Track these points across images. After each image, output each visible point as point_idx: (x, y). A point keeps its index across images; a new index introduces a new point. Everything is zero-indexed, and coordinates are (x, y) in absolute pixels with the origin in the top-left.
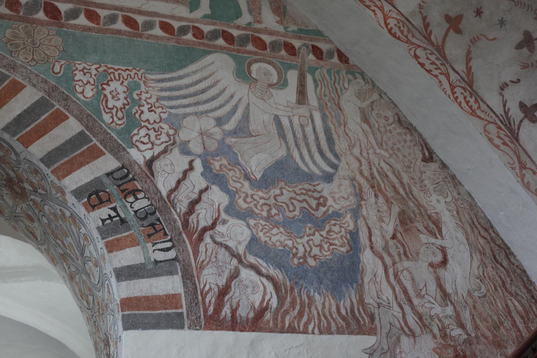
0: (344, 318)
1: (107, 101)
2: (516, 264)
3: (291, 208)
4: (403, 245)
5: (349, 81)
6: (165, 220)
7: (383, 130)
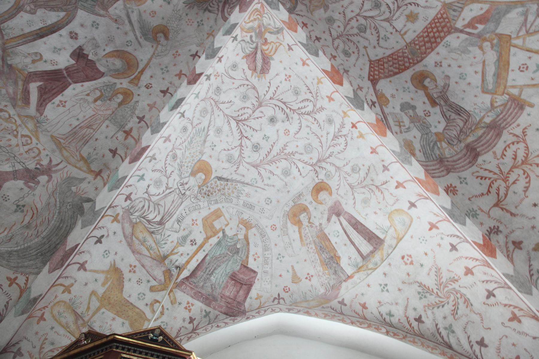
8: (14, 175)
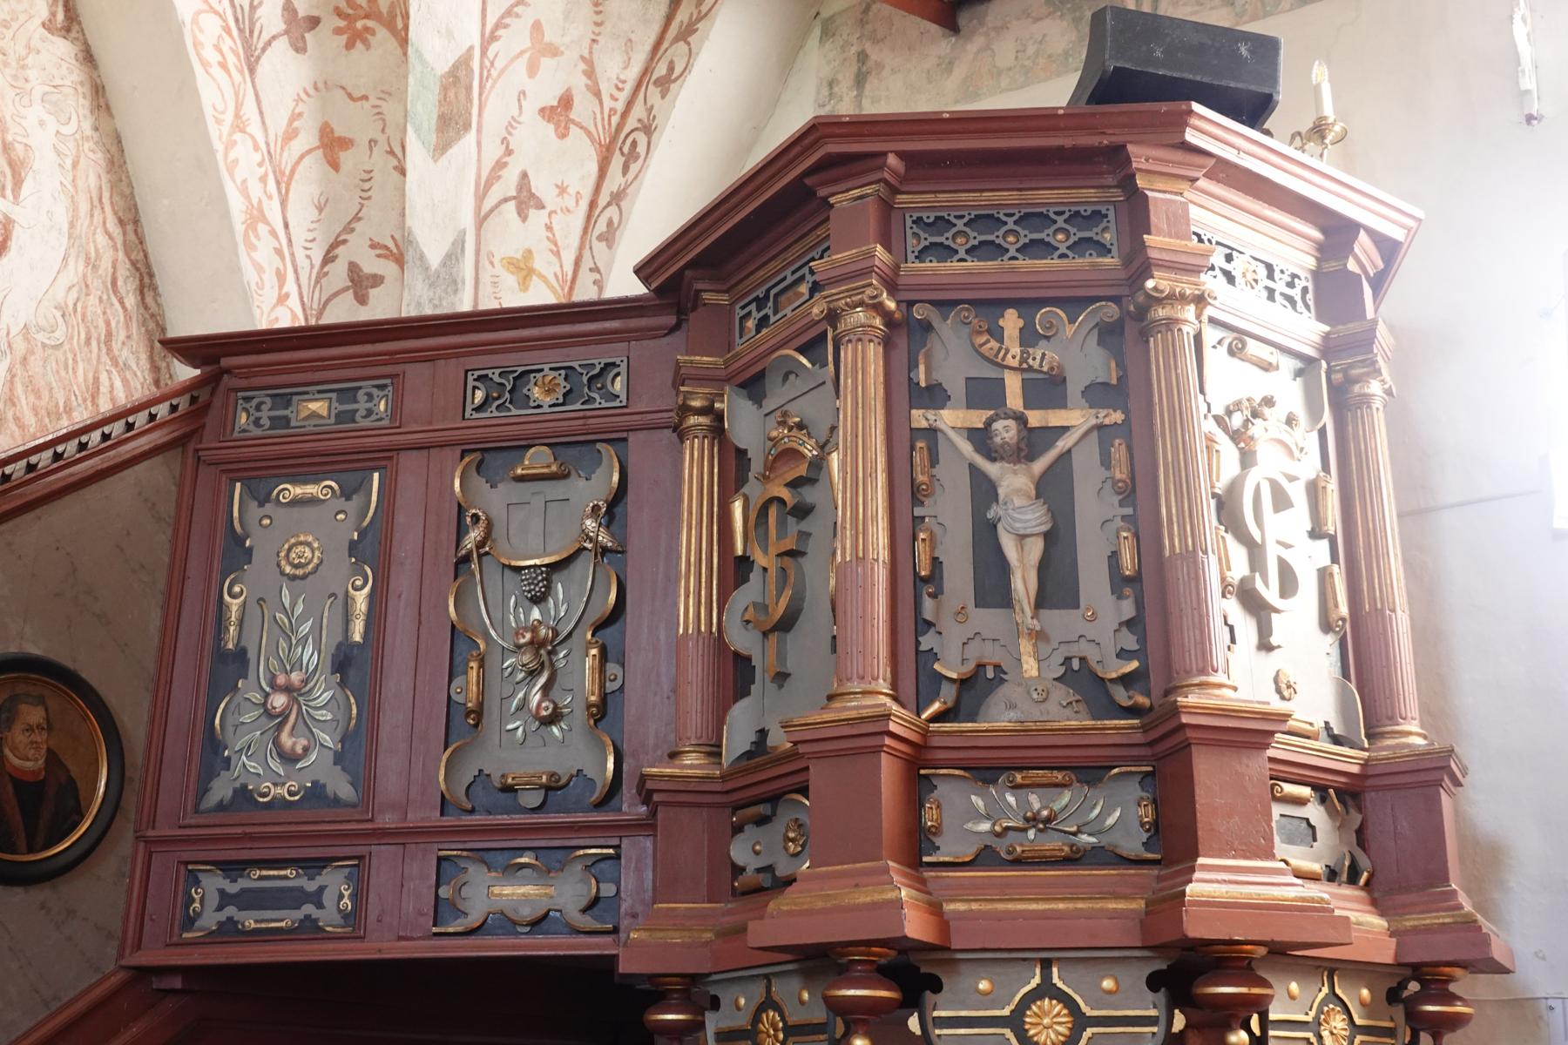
2: (152, 310)
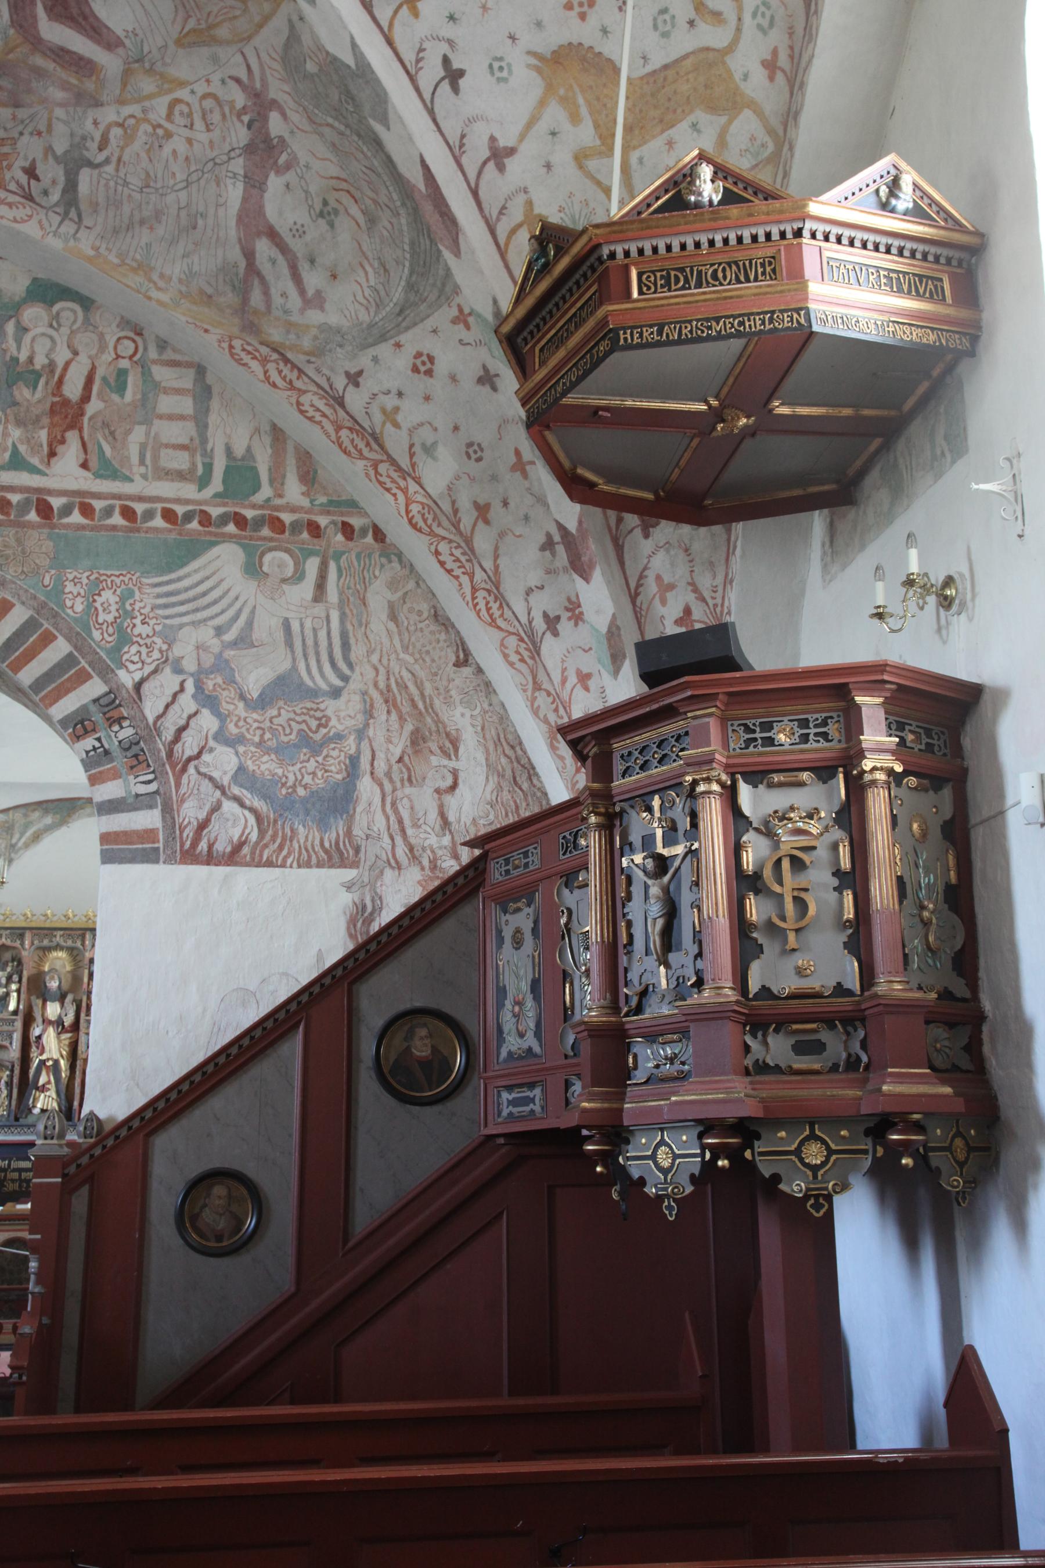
0: (326, 851)
1: (97, 615)
3: (288, 731)
4: (408, 769)
5: (382, 566)
6: (149, 750)
7: (412, 628)
8: (254, 186)
